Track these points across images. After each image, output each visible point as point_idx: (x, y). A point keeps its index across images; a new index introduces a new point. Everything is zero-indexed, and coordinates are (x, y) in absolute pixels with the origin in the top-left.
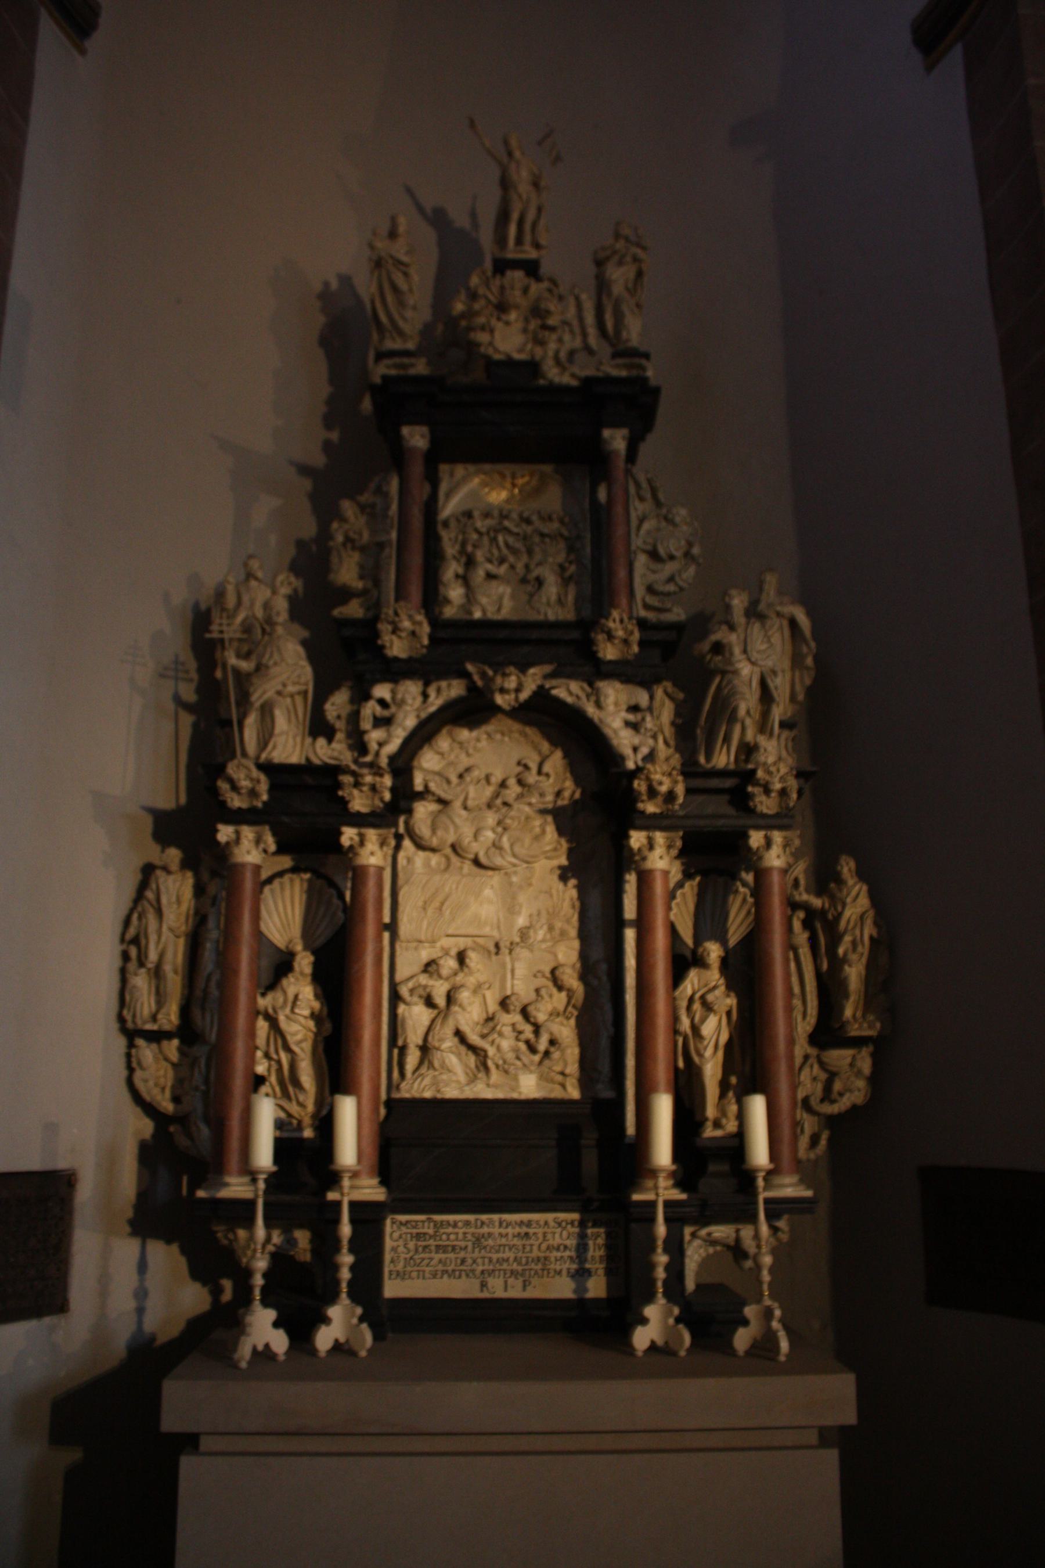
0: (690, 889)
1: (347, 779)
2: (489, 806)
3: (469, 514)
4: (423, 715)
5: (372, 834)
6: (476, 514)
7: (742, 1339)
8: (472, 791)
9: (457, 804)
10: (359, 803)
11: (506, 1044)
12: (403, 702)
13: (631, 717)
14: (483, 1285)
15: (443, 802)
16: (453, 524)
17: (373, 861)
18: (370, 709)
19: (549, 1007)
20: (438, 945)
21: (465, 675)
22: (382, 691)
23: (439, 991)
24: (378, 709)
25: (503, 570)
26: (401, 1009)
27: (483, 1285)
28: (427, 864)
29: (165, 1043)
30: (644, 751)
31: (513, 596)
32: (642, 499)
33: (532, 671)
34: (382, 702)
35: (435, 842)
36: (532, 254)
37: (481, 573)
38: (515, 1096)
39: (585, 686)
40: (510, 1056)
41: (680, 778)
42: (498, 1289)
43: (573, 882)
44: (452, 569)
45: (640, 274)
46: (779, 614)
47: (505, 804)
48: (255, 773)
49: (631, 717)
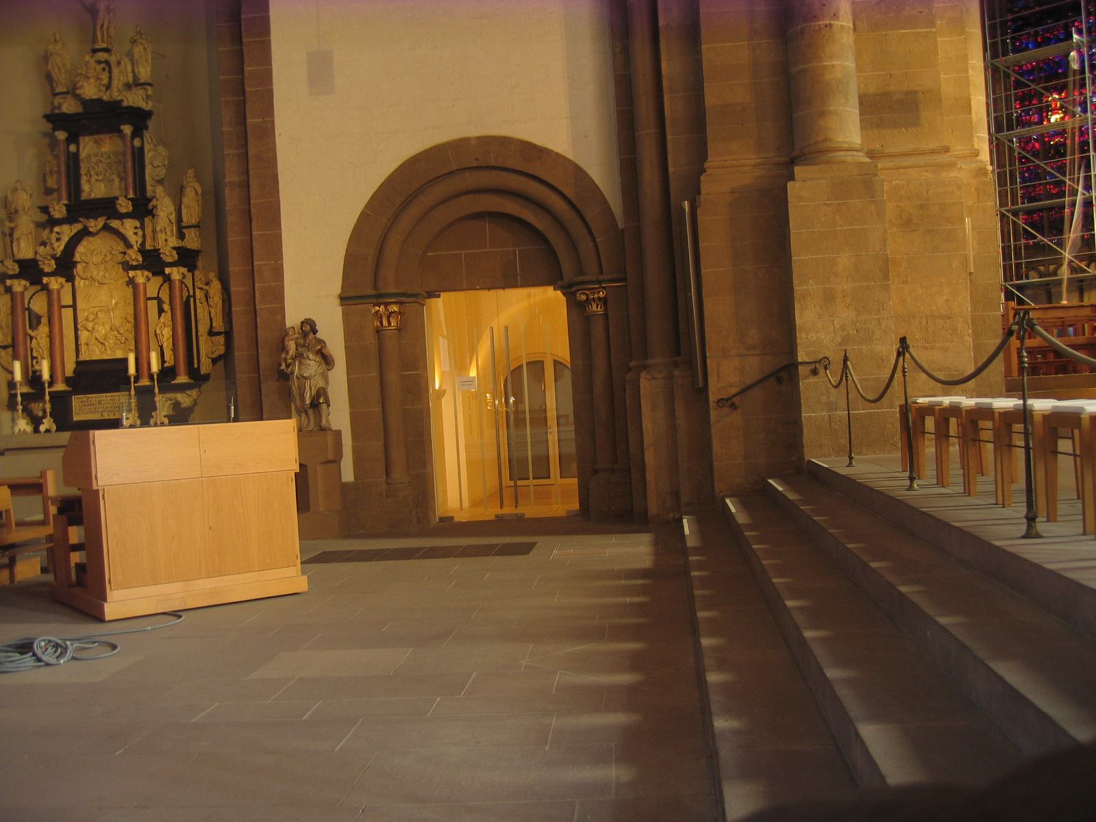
0: (166, 286)
1: (40, 263)
2: (102, 263)
3: (90, 156)
4: (70, 236)
5: (52, 279)
6: (92, 156)
7: (152, 422)
8: (95, 259)
9: (91, 263)
10: (47, 270)
11: (111, 341)
12: (63, 233)
13: (136, 231)
14: (102, 415)
15: (85, 262)
16: (85, 161)
17: (55, 287)
18: (54, 236)
19: (126, 328)
20: (90, 310)
21: (81, 222)
22: (56, 229)
23: (90, 325)
24: (57, 235)
25: (100, 178)
26: (79, 332)
27: (102, 415)
28: (84, 284)
29: (8, 349)
30: (139, 242)
31: (105, 187)
32: (149, 144)
33: (99, 219)
34: (57, 233)
35: (84, 277)
36: (104, 45)
37: (93, 180)
38: (115, 357)
39: (120, 221)
40: (113, 345)
41: (139, 254)
42: (106, 417)
43: (130, 286)
44: (84, 180)
45: (145, 49)
47: (107, 262)
48: (12, 263)
49: (136, 231)
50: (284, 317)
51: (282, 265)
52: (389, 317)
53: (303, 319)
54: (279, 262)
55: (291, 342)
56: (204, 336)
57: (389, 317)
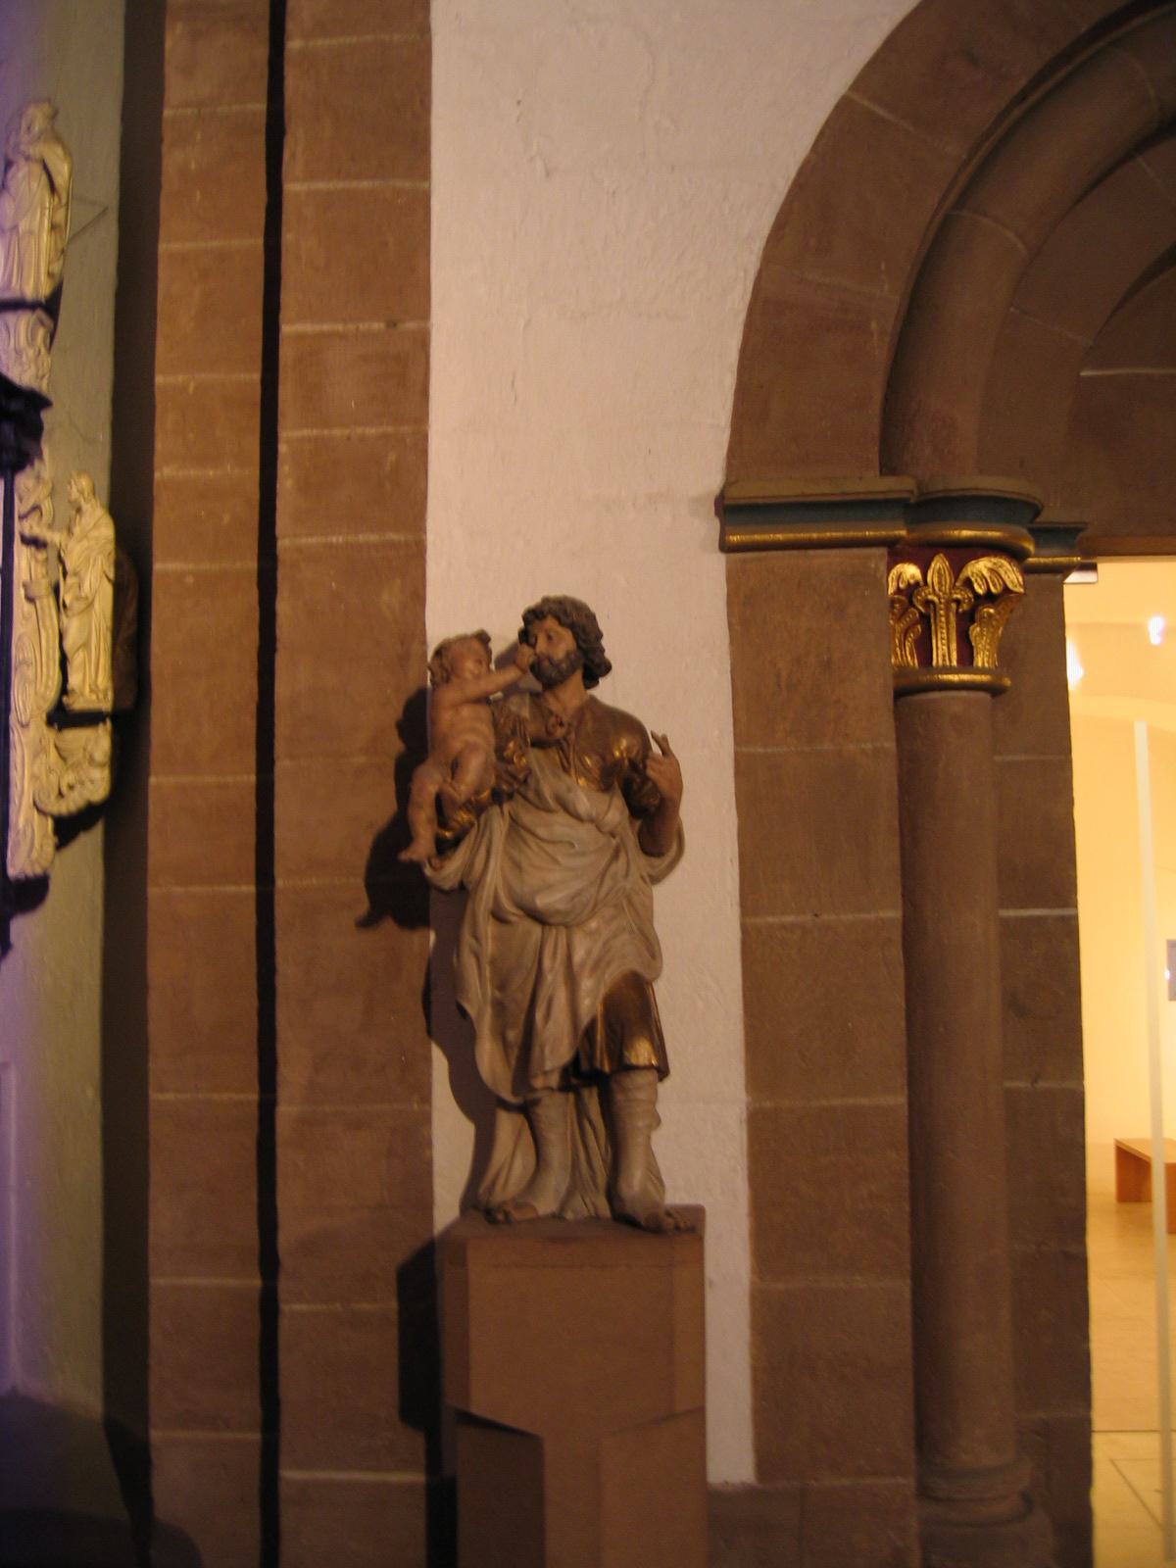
46: (28, 158)
50: (417, 597)
51: (423, 342)
52: (966, 620)
53: (533, 600)
54: (411, 325)
55: (466, 712)
56: (32, 726)
57: (966, 620)
